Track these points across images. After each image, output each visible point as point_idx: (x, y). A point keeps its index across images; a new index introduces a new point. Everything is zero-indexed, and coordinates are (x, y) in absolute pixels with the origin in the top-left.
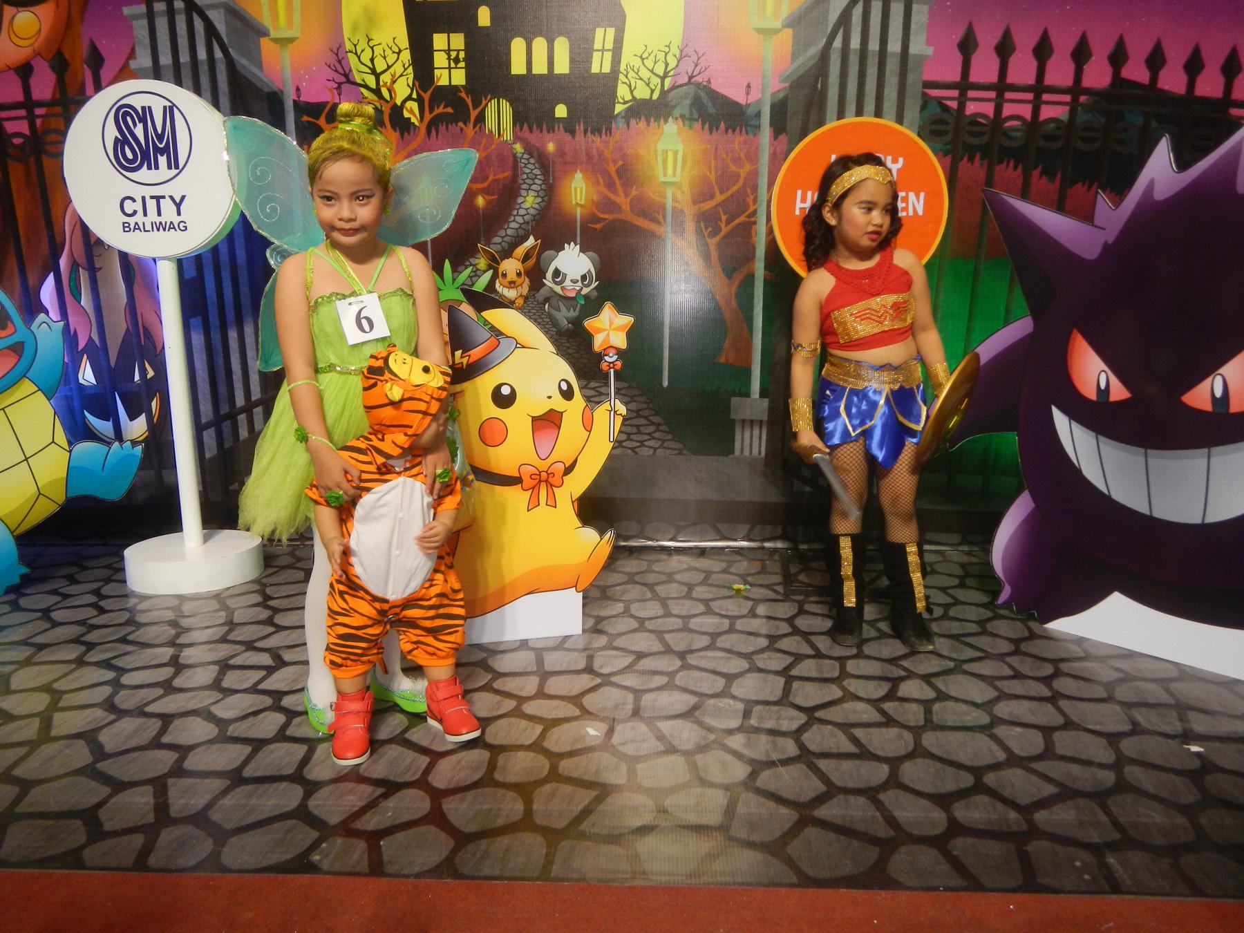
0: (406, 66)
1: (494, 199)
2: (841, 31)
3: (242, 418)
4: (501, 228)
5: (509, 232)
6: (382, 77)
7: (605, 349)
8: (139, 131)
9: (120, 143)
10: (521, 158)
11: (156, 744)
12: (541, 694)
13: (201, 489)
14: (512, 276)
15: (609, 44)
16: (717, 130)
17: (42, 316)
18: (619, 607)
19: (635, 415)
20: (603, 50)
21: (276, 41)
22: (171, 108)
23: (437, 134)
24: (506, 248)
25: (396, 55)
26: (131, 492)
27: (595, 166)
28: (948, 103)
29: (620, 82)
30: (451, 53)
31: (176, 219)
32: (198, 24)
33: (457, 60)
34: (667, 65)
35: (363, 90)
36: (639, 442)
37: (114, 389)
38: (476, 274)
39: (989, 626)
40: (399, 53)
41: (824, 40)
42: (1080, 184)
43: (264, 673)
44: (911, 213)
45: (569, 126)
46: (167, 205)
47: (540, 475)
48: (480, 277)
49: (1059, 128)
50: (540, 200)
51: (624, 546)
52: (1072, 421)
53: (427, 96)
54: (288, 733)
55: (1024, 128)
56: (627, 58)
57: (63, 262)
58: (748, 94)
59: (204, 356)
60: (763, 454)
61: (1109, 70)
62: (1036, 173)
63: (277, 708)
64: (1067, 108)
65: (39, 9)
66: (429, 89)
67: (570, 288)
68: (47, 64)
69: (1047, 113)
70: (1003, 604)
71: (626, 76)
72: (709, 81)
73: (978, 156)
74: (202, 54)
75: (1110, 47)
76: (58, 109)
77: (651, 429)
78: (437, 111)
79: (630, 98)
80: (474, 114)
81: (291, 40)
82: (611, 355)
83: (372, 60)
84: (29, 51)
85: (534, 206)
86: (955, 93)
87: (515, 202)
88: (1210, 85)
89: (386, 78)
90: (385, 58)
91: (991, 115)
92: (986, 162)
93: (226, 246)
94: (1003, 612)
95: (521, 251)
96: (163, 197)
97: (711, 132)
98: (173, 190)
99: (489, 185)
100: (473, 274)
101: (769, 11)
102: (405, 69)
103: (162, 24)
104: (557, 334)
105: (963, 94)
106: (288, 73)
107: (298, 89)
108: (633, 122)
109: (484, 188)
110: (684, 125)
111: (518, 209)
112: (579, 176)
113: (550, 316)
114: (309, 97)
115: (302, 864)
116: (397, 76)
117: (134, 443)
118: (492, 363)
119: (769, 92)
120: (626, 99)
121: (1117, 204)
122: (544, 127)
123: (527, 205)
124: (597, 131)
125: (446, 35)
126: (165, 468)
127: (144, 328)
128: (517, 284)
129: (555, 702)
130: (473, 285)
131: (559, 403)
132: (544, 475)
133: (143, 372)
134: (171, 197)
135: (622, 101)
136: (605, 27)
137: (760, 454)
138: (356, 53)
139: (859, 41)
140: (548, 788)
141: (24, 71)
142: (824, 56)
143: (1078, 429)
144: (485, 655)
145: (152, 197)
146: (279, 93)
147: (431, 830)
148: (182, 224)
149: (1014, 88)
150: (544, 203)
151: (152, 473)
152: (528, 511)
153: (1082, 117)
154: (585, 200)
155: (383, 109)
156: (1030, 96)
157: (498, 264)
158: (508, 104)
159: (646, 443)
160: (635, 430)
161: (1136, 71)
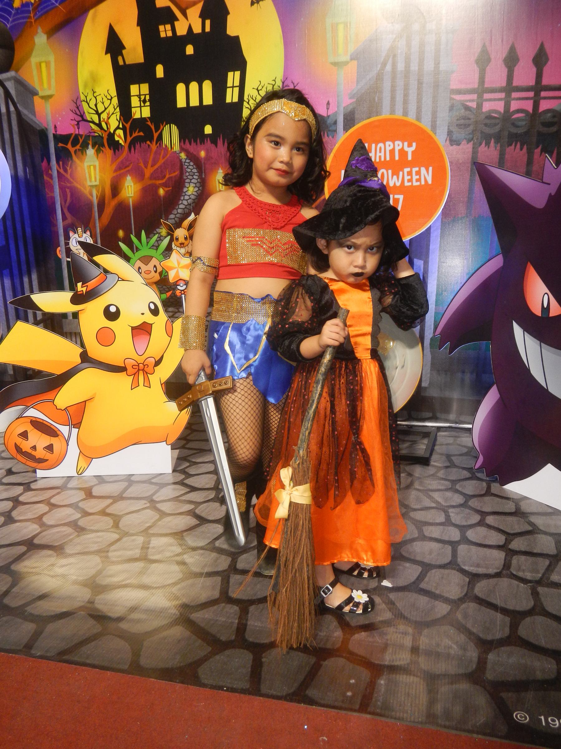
4: (175, 209)
7: (177, 281)
10: (185, 162)
15: (237, 83)
20: (233, 87)
21: (43, 97)
24: (178, 221)
29: (244, 107)
30: (141, 97)
33: (144, 101)
35: (92, 125)
38: (160, 239)
40: (111, 100)
41: (379, 66)
44: (423, 183)
45: (213, 138)
47: (139, 366)
48: (163, 241)
49: (554, 117)
50: (197, 189)
52: (525, 332)
53: (128, 126)
56: (249, 91)
58: (328, 109)
62: (538, 150)
69: (544, 106)
70: (480, 468)
71: (248, 103)
73: (493, 141)
81: (50, 97)
82: (181, 285)
83: (96, 105)
86: (475, 96)
87: (183, 192)
89: (104, 116)
90: (103, 103)
91: (502, 111)
94: (479, 475)
99: (166, 182)
100: (159, 239)
101: (341, 50)
102: (115, 110)
106: (49, 118)
107: (55, 127)
109: (163, 183)
111: (184, 196)
114: (62, 131)
118: (102, 291)
119: (343, 105)
122: (198, 141)
123: (189, 193)
125: (138, 85)
128: (185, 245)
131: (149, 318)
132: (141, 365)
136: (234, 70)
138: (87, 102)
142: (379, 77)
143: (528, 337)
146: (45, 129)
149: (519, 89)
150: (200, 191)
152: (132, 389)
155: (103, 136)
156: (531, 94)
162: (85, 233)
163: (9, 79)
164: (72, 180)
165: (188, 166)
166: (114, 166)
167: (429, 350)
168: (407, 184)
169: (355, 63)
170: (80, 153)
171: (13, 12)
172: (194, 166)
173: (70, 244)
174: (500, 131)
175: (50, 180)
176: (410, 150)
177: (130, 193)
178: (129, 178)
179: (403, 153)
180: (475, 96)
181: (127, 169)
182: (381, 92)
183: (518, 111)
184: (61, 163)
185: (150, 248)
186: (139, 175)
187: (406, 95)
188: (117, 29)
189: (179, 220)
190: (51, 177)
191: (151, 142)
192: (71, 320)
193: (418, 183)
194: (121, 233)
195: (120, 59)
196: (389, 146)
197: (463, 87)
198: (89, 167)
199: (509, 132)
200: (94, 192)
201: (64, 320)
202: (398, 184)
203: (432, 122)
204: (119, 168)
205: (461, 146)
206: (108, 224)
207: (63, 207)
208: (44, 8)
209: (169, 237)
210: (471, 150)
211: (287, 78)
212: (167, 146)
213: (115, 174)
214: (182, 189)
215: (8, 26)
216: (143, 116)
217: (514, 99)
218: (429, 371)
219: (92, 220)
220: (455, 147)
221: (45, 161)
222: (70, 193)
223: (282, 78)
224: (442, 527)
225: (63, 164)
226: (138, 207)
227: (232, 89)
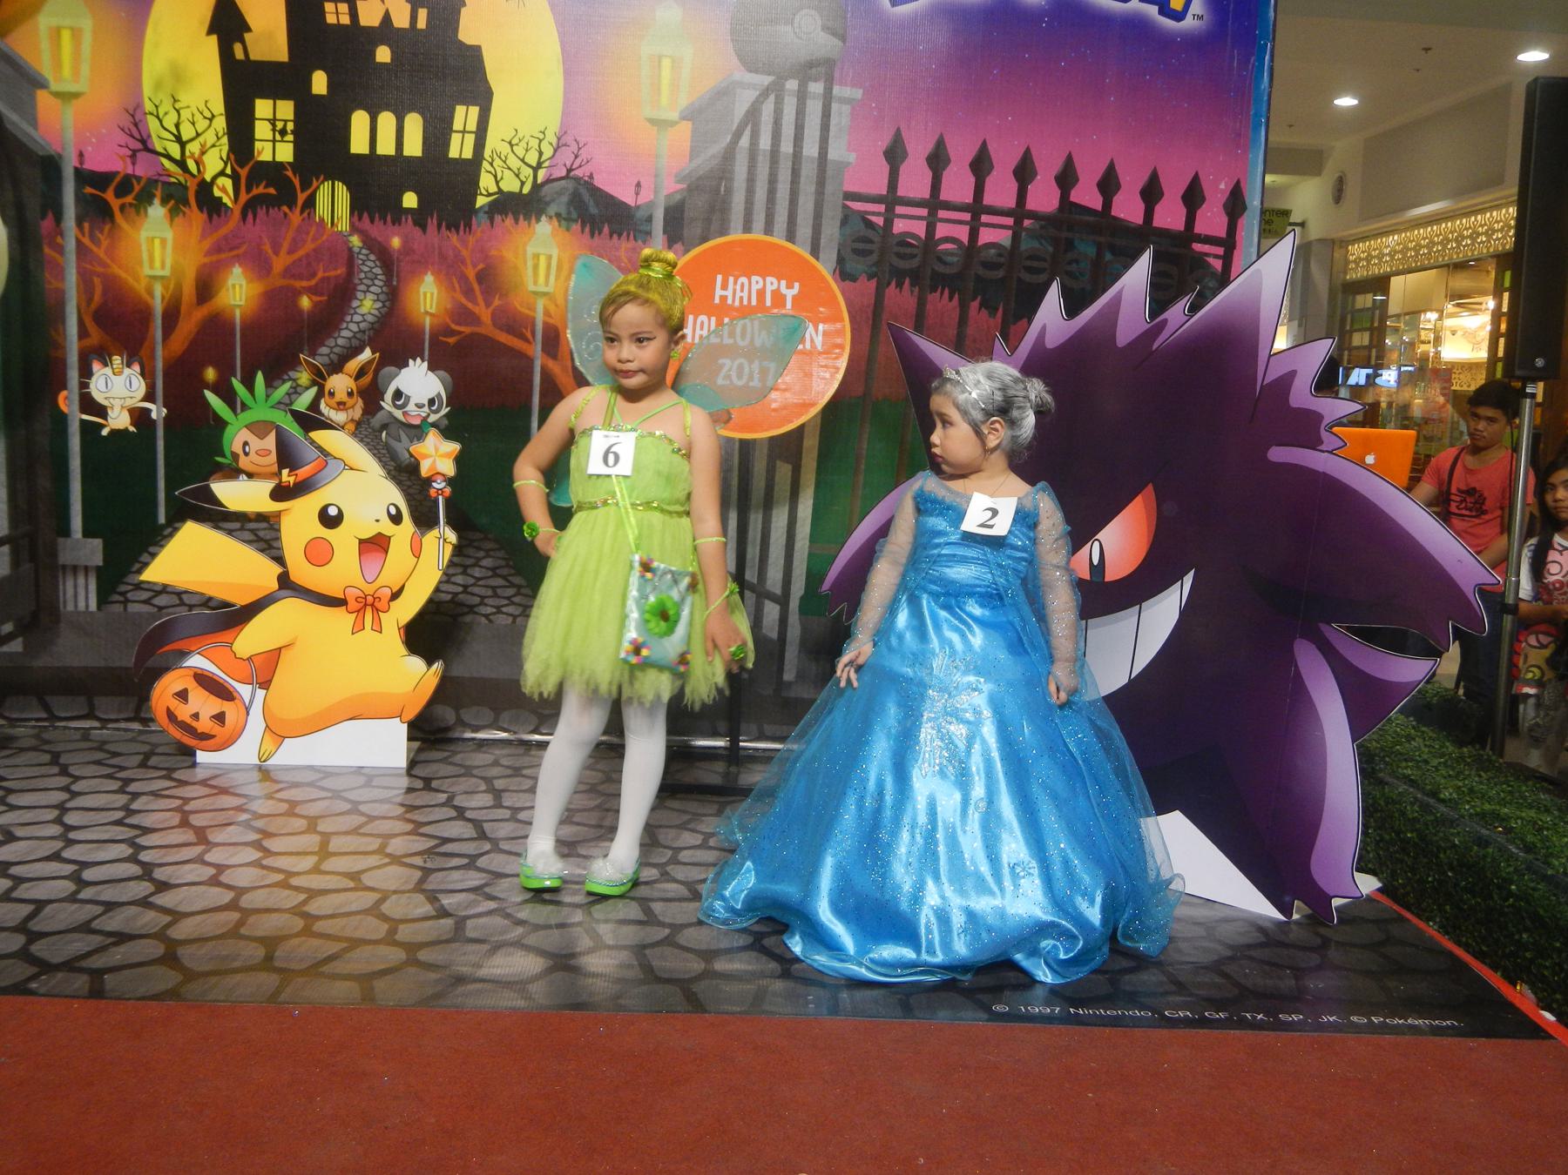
0: (220, 135)
1: (321, 301)
2: (749, 128)
4: (329, 336)
5: (340, 341)
6: (189, 147)
10: (359, 253)
12: (316, 870)
14: (341, 395)
15: (472, 125)
16: (600, 234)
18: (442, 797)
19: (490, 573)
20: (464, 132)
21: (57, 95)
23: (254, 220)
25: (208, 121)
27: (449, 269)
28: (873, 218)
29: (483, 170)
30: (277, 123)
33: (283, 132)
34: (541, 154)
35: (165, 162)
36: (492, 606)
38: (296, 391)
40: (211, 120)
41: (729, 138)
42: (1025, 320)
44: (808, 346)
48: (300, 394)
49: (1000, 255)
50: (379, 305)
51: (473, 739)
53: (244, 172)
54: (15, 895)
55: (960, 252)
56: (493, 142)
58: (637, 194)
61: (1058, 193)
62: (975, 304)
66: (247, 164)
67: (414, 414)
69: (986, 236)
72: (591, 176)
73: (907, 281)
75: (1057, 166)
77: (510, 592)
78: (255, 191)
79: (496, 190)
81: (76, 95)
83: (177, 126)
85: (373, 312)
86: (882, 208)
88: (1169, 216)
89: (193, 148)
90: (193, 124)
91: (923, 237)
95: (353, 365)
97: (592, 235)
99: (316, 285)
101: (664, 100)
104: (395, 469)
105: (890, 210)
107: (81, 155)
108: (498, 218)
110: (560, 225)
112: (429, 279)
113: (387, 446)
114: (94, 164)
115: (20, 989)
116: (209, 145)
119: (664, 192)
120: (491, 191)
122: (389, 218)
123: (364, 310)
124: (453, 226)
125: (271, 102)
129: (328, 877)
130: (291, 403)
135: (485, 193)
138: (158, 117)
139: (769, 142)
142: (729, 155)
147: (160, 970)
149: (948, 206)
153: (1026, 245)
154: (437, 307)
156: (967, 216)
157: (325, 380)
158: (345, 188)
159: (504, 609)
160: (490, 593)
161: (1087, 195)
162: (129, 366)
164: (109, 261)
165: (364, 261)
166: (207, 244)
167: (797, 617)
169: (689, 124)
170: (133, 210)
172: (378, 263)
173: (92, 386)
174: (919, 267)
176: (790, 294)
177: (238, 298)
178: (237, 271)
179: (779, 298)
182: (731, 180)
183: (947, 239)
184: (86, 225)
185: (272, 407)
186: (259, 265)
187: (772, 192)
189: (339, 361)
190: (60, 250)
191: (290, 209)
192: (78, 540)
194: (210, 374)
196: (757, 282)
197: (864, 190)
198: (151, 240)
199: (933, 269)
200: (158, 290)
201: (61, 540)
203: (813, 238)
204: (217, 249)
205: (858, 283)
206: (184, 354)
207: (82, 311)
211: (565, 133)
212: (323, 219)
213: (206, 260)
216: (278, 159)
217: (942, 220)
218: (797, 652)
219: (147, 344)
220: (847, 282)
221: (50, 215)
222: (101, 287)
223: (557, 131)
226: (251, 327)
227: (461, 135)
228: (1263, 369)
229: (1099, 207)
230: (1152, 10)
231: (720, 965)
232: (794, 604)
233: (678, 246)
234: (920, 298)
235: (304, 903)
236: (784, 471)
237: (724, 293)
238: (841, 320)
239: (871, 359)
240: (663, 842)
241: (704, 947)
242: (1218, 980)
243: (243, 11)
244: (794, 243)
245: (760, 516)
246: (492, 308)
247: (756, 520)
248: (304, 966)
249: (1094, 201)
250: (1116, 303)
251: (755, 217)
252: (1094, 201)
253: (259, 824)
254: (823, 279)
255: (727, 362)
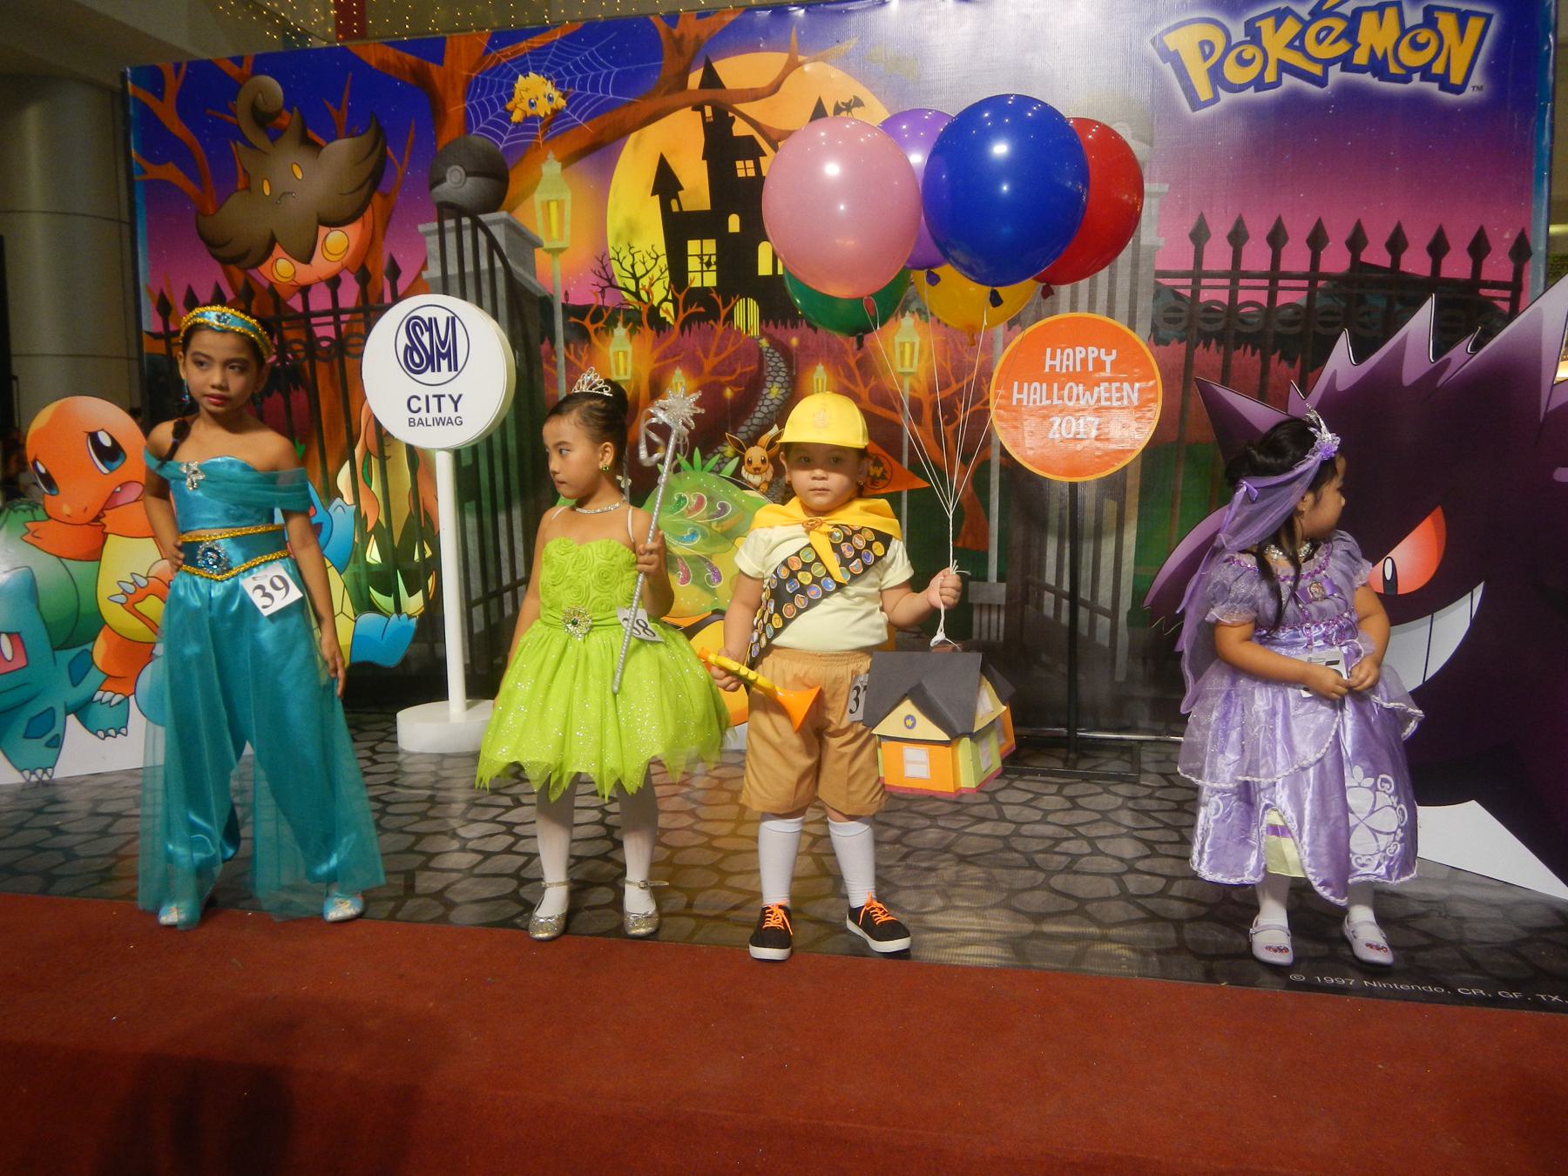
3: (508, 595)
8: (426, 339)
9: (410, 349)
10: (767, 352)
11: (410, 850)
12: (733, 834)
13: (468, 662)
14: (757, 463)
17: (338, 500)
21: (549, 251)
22: (453, 319)
26: (405, 661)
28: (1181, 291)
31: (453, 415)
32: (482, 238)
33: (709, 264)
37: (397, 566)
38: (724, 461)
39: (1186, 807)
40: (656, 259)
43: (503, 810)
44: (1125, 402)
46: (446, 402)
48: (727, 463)
49: (1297, 313)
50: (784, 391)
53: (681, 297)
54: (514, 849)
57: (358, 451)
59: (476, 538)
60: (1001, 639)
62: (1276, 356)
63: (510, 832)
64: (1306, 293)
65: (349, 228)
68: (353, 276)
69: (1283, 298)
73: (1214, 341)
74: (484, 265)
75: (1347, 233)
76: (361, 316)
78: (690, 311)
80: (723, 313)
81: (561, 250)
83: (633, 266)
84: (340, 263)
86: (1189, 282)
88: (1457, 266)
89: (644, 282)
91: (1227, 303)
92: (1222, 348)
93: (499, 436)
96: (444, 396)
98: (452, 389)
99: (736, 379)
103: (451, 239)
105: (1196, 281)
106: (558, 280)
107: (566, 294)
112: (820, 368)
114: (577, 300)
117: (410, 617)
121: (1306, 393)
123: (772, 396)
126: (437, 641)
127: (425, 512)
133: (422, 552)
134: (451, 396)
137: (998, 636)
140: (711, 892)
141: (334, 282)
144: (694, 806)
145: (435, 396)
148: (458, 420)
151: (426, 645)
153: (1321, 302)
156: (1266, 283)
157: (744, 451)
161: (1376, 254)
163: (495, 222)
166: (656, 354)
167: (1126, 627)
168: (1103, 403)
171: (510, 128)
175: (554, 371)
176: (1108, 360)
178: (678, 372)
179: (1099, 365)
180: (1189, 282)
181: (677, 358)
183: (1248, 304)
186: (694, 368)
188: (671, 161)
190: (555, 365)
191: (716, 322)
193: (1119, 403)
195: (674, 204)
198: (617, 354)
202: (1092, 402)
204: (663, 357)
208: (561, 125)
209: (737, 459)
210: (1183, 352)
213: (657, 365)
214: (762, 389)
215: (501, 147)
220: (1162, 347)
221: (547, 341)
224: (1178, 846)
225: (575, 349)
228: (1547, 398)
229: (1389, 266)
230: (1433, 87)
231: (1050, 928)
232: (1123, 617)
233: (1017, 327)
234: (1224, 355)
235: (722, 860)
236: (1111, 506)
237: (1053, 363)
238: (1153, 378)
239: (1183, 408)
240: (1008, 817)
241: (1033, 909)
242: (1512, 960)
243: (677, 173)
244: (1113, 318)
245: (1091, 546)
246: (869, 388)
247: (1087, 549)
248: (715, 912)
249: (1385, 260)
250: (1400, 350)
251: (1080, 299)
252: (1385, 260)
253: (699, 795)
254: (1136, 345)
255: (1058, 420)
